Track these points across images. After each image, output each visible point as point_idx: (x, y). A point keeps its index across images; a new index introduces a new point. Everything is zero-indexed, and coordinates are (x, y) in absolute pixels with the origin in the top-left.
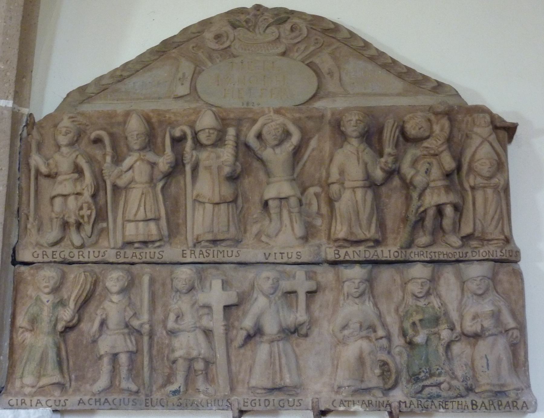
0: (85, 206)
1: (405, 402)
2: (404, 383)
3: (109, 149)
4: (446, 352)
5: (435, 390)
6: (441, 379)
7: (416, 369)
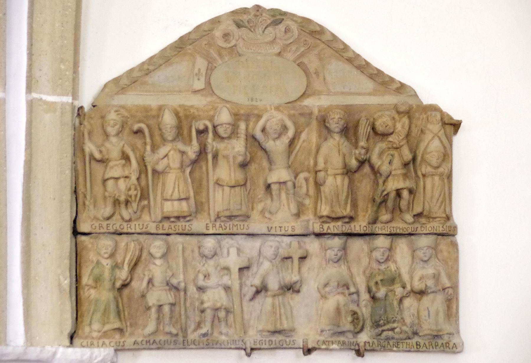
1: (369, 343)
2: (369, 329)
4: (399, 305)
5: (390, 333)
6: (395, 325)
7: (377, 318)
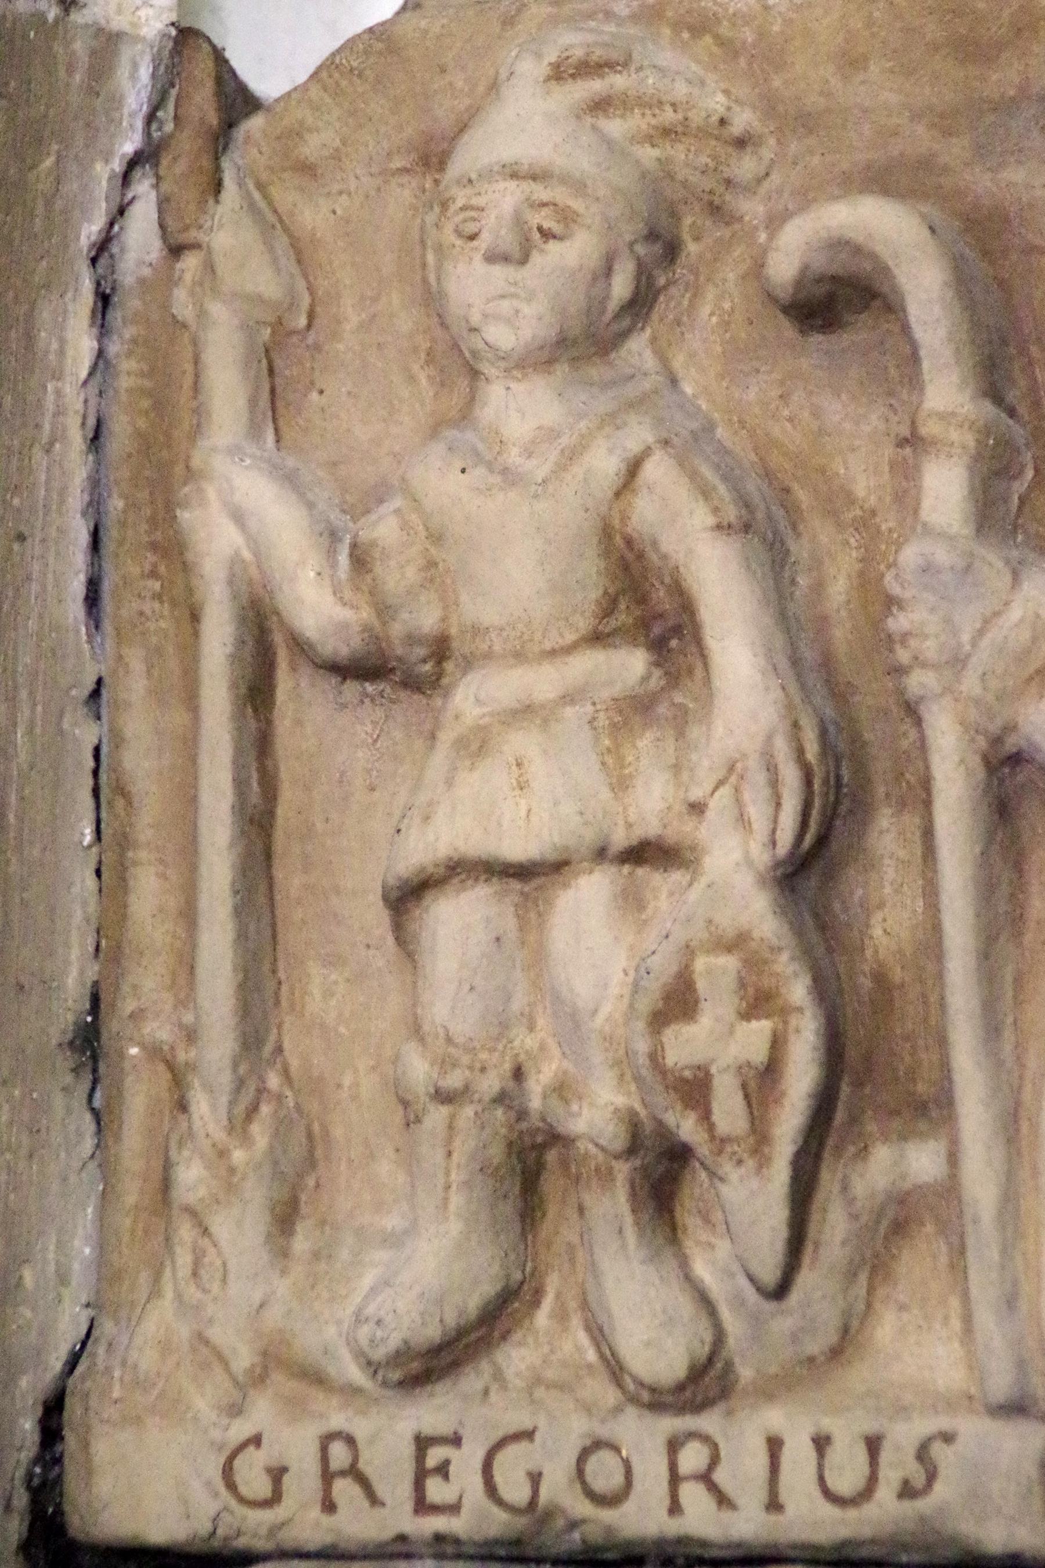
0: (717, 975)
3: (947, 393)
